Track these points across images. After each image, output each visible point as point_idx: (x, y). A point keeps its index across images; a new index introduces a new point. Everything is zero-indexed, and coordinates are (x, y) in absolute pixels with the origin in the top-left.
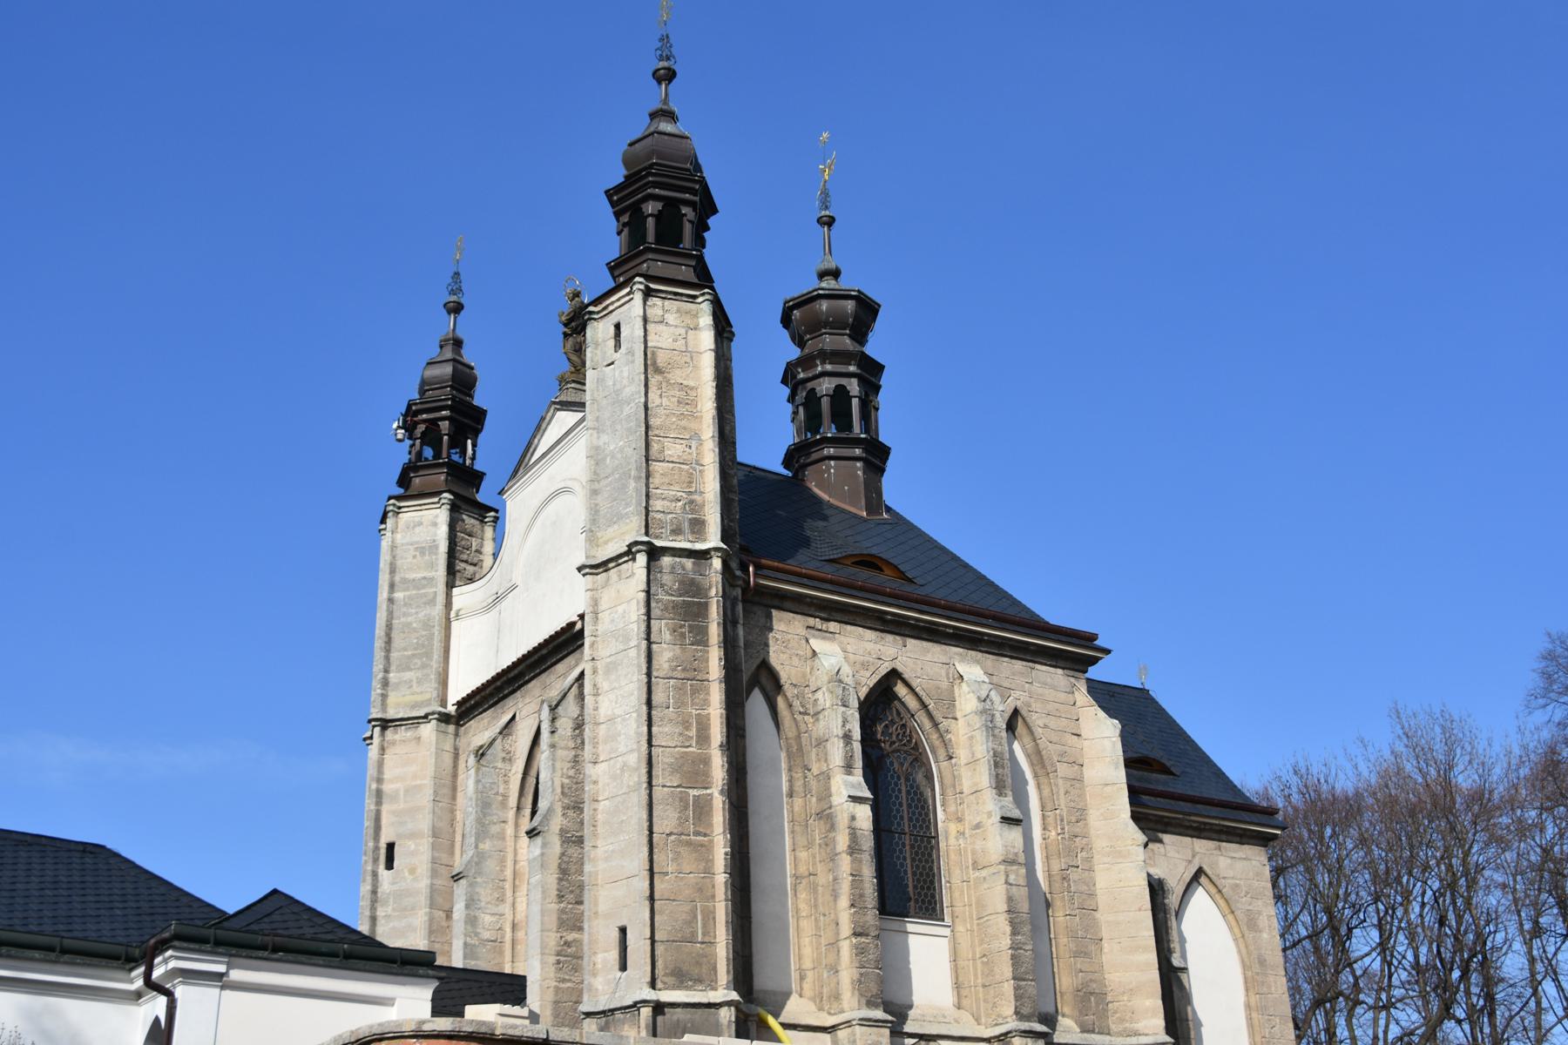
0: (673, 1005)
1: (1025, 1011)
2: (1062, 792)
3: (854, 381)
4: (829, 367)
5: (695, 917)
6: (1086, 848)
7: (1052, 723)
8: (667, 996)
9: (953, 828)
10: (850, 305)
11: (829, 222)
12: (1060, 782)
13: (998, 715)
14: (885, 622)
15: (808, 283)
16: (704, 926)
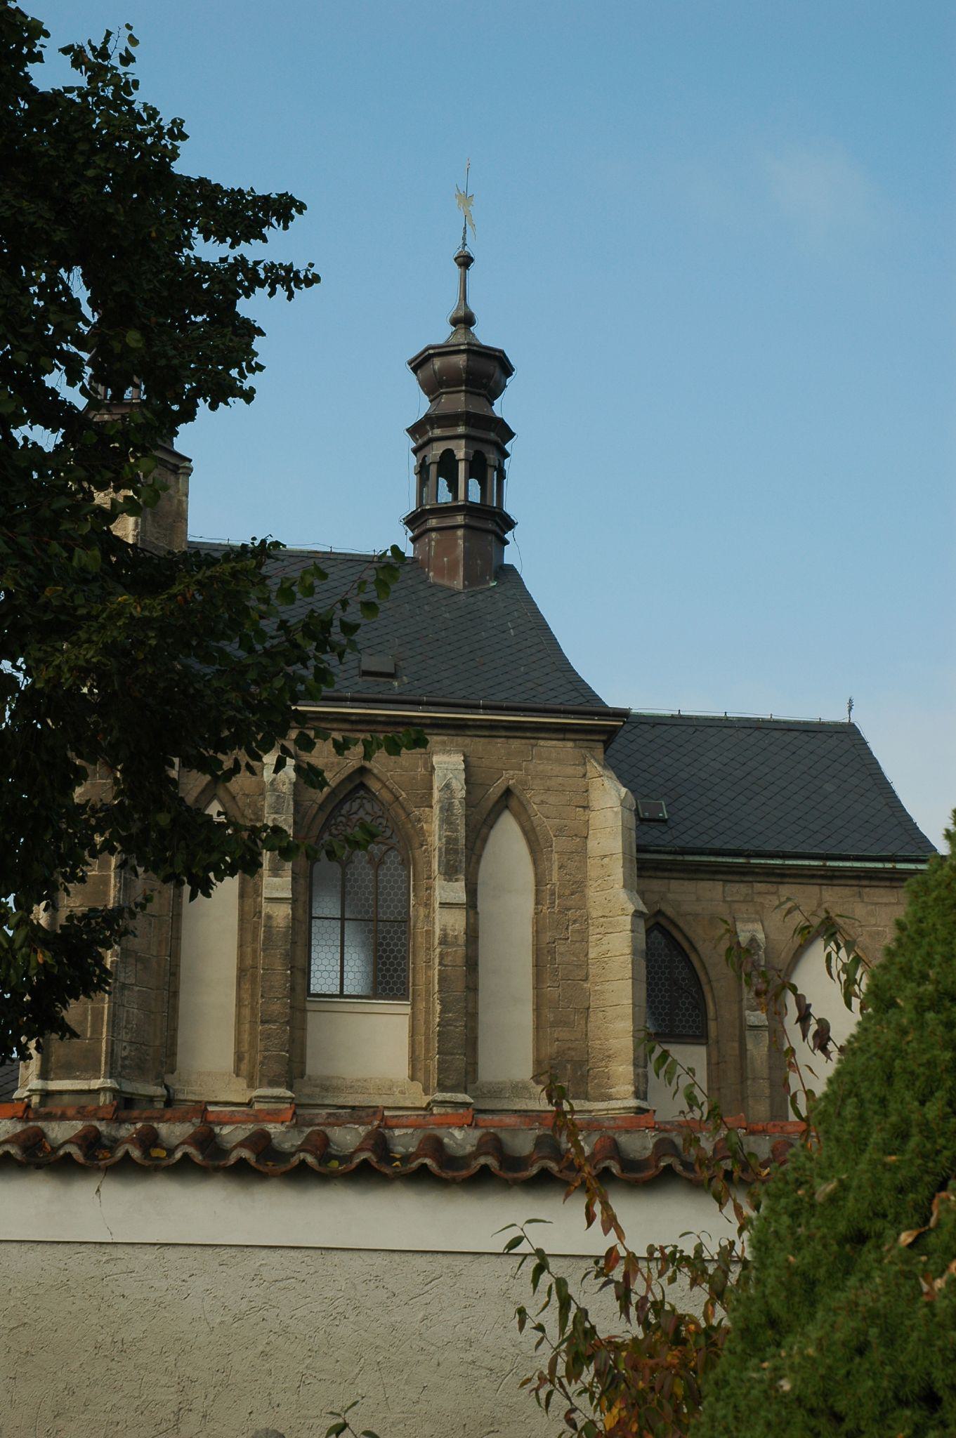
0: (61, 1092)
1: (449, 1083)
2: (555, 867)
3: (463, 442)
4: (438, 432)
5: (86, 1019)
6: (586, 919)
7: (552, 799)
8: (54, 1085)
9: (422, 911)
10: (461, 360)
11: (465, 261)
12: (555, 856)
13: (456, 802)
14: (352, 722)
15: (442, 333)
16: (93, 1026)
